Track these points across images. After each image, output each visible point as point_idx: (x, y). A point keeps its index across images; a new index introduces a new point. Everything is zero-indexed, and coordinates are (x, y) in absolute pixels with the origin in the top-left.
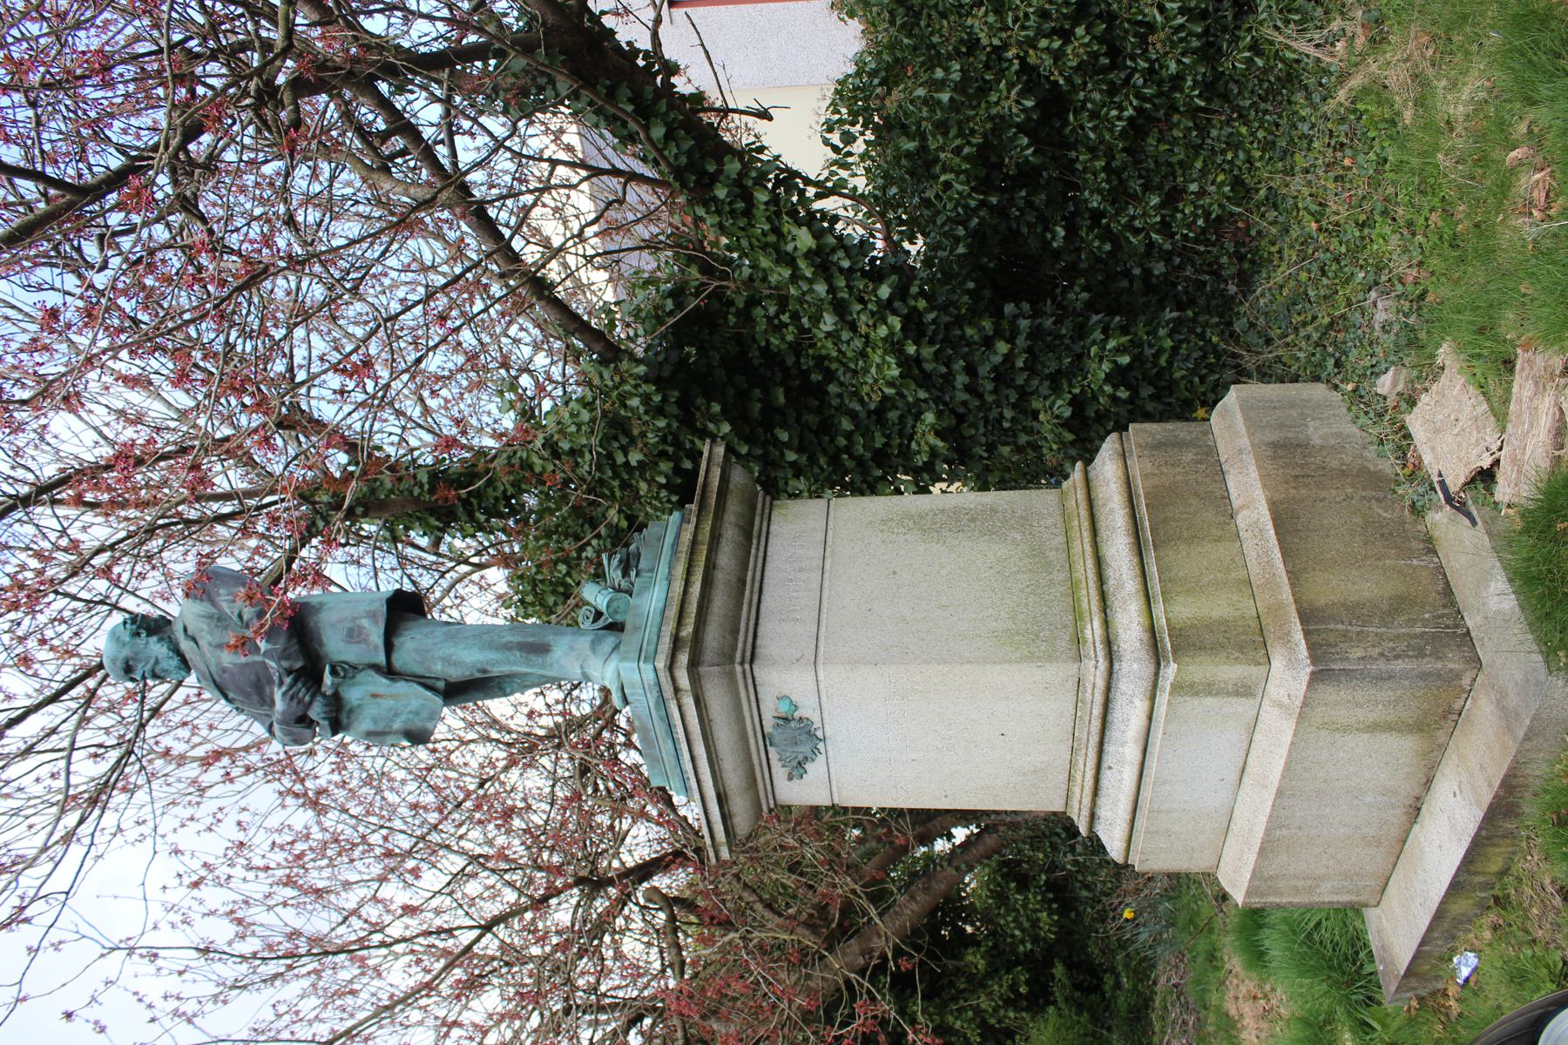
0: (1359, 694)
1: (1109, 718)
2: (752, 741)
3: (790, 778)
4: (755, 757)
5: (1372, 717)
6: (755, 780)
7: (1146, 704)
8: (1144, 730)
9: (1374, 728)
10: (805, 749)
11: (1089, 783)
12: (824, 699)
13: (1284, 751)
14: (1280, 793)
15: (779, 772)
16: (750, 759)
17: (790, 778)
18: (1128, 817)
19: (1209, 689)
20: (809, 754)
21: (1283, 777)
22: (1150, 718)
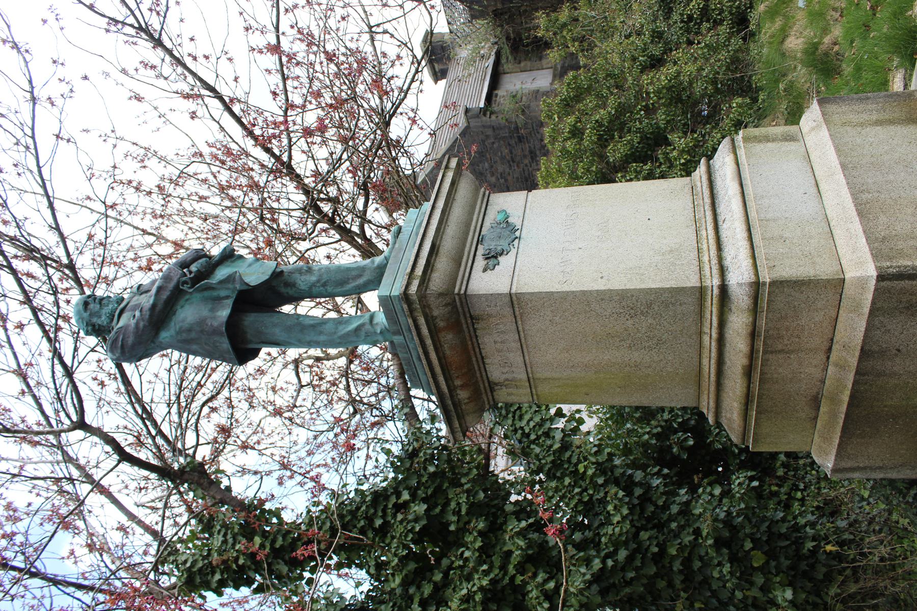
0: (856, 108)
1: (715, 191)
2: (471, 234)
3: (485, 270)
4: (468, 245)
5: (874, 117)
6: (461, 258)
7: (732, 156)
8: (736, 173)
9: (879, 123)
10: (503, 244)
11: (712, 241)
12: (527, 211)
13: (830, 143)
14: (844, 167)
15: (480, 263)
16: (464, 245)
17: (485, 270)
18: (745, 235)
19: (767, 139)
20: (506, 247)
21: (839, 156)
22: (737, 164)
